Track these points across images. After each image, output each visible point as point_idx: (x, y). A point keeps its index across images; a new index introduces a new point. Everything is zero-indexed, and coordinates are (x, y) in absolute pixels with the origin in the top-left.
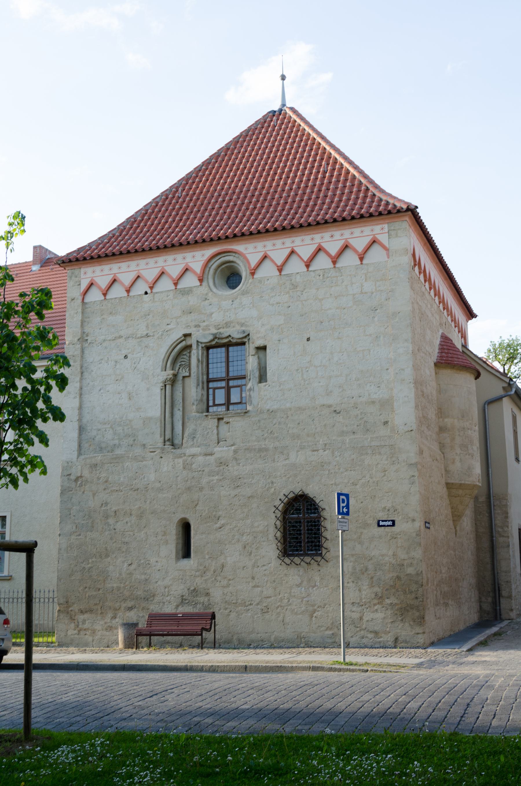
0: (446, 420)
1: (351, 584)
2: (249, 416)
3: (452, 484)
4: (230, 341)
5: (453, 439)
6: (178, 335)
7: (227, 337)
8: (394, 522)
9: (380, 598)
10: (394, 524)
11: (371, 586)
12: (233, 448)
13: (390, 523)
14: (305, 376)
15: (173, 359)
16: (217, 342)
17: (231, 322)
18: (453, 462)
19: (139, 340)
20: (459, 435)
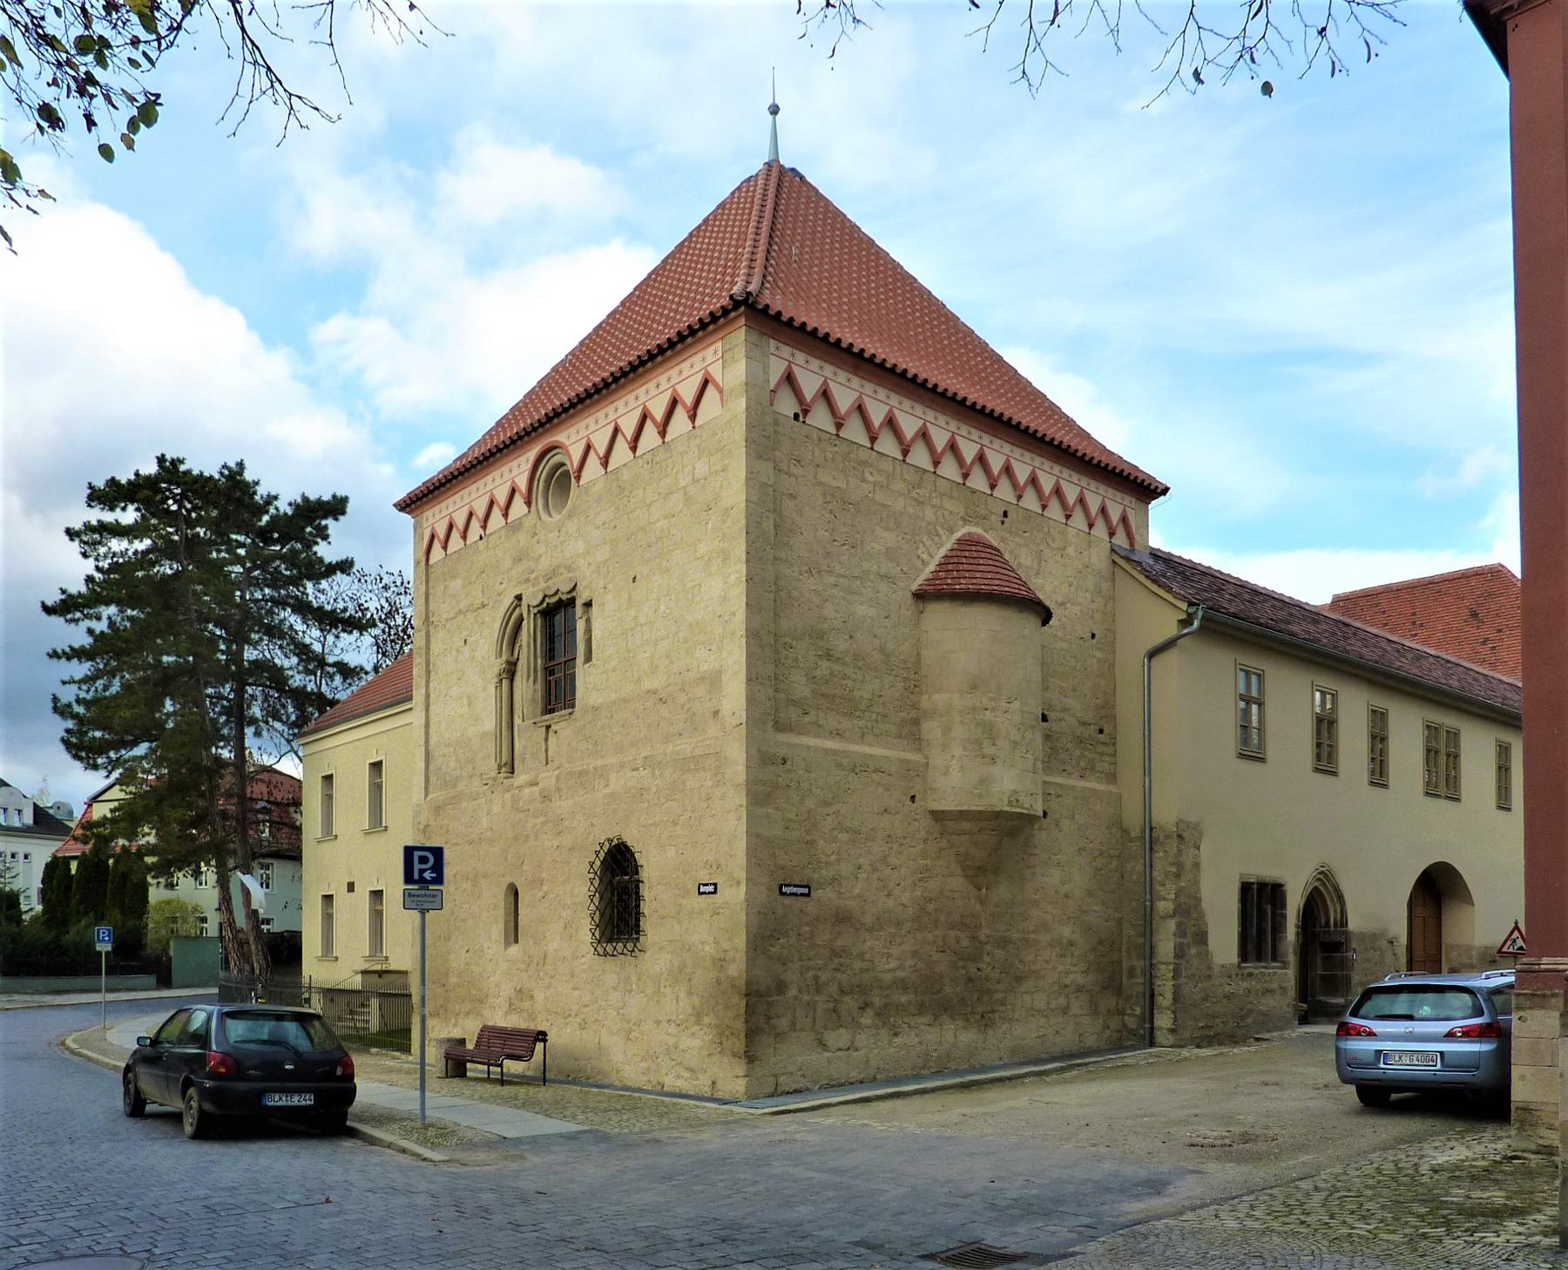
0: (936, 696)
1: (668, 990)
2: (575, 719)
3: (943, 811)
4: (560, 600)
5: (947, 730)
6: (508, 600)
7: (557, 593)
8: (715, 885)
9: (698, 1015)
10: (715, 892)
11: (689, 993)
12: (556, 772)
13: (711, 889)
14: (630, 645)
15: (510, 637)
16: (548, 604)
17: (558, 567)
18: (946, 773)
19: (475, 614)
20: (962, 722)
